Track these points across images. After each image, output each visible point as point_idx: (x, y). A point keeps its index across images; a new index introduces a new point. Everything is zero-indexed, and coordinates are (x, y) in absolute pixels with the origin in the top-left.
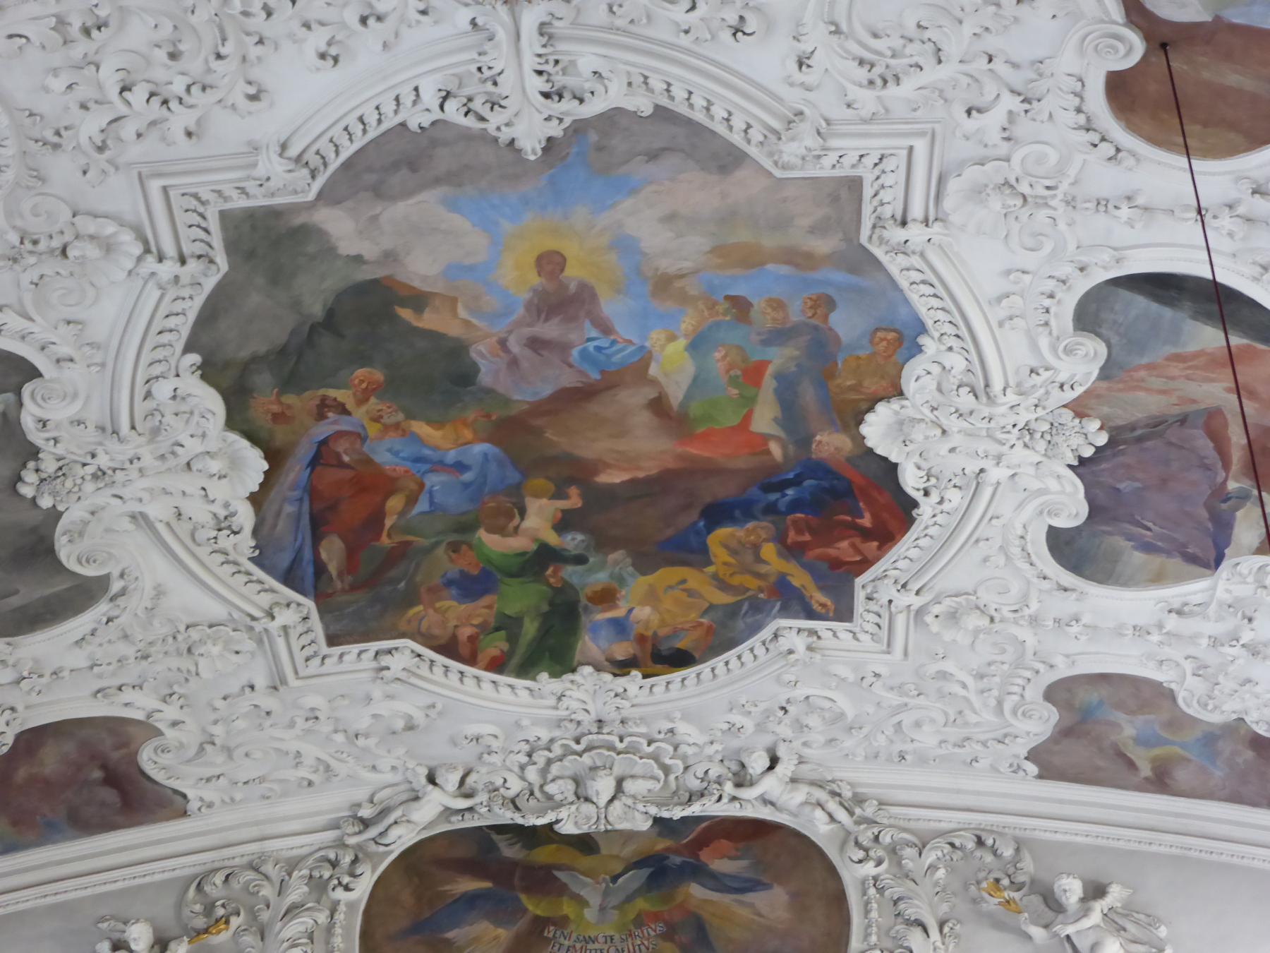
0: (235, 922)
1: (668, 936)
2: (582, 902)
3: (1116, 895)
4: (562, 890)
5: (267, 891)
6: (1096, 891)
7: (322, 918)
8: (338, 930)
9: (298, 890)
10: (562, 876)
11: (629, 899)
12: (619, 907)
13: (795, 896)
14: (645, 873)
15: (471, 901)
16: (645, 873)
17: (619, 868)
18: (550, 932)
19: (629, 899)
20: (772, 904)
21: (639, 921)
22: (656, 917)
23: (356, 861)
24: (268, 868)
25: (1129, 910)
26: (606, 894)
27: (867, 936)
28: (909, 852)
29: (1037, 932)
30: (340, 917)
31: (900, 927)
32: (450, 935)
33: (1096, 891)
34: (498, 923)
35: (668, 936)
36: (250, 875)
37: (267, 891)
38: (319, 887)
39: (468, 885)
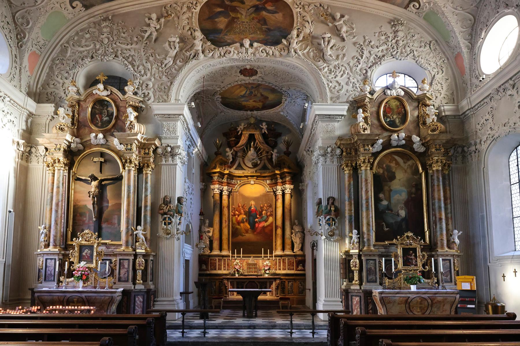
0: (173, 15)
1: (259, 22)
2: (242, 14)
3: (346, 17)
4: (238, 12)
5: (179, 9)
6: (342, 16)
7: (190, 15)
8: (193, 18)
9: (185, 9)
10: (237, 8)
11: (251, 14)
12: (249, 16)
13: (283, 15)
14: (254, 9)
15: (220, 13)
16: (254, 9)
17: (249, 7)
18: (236, 20)
19: (251, 14)
20: (279, 16)
21: (253, 19)
22: (257, 18)
23: (196, 3)
24: (179, 4)
25: (348, 20)
26: (246, 13)
27: (297, 23)
28: (306, 7)
29: (330, 24)
30: (194, 15)
31: (304, 22)
32: (216, 20)
33: (342, 16)
34: (225, 18)
35: (259, 22)
36: (175, 5)
37: (179, 9)
38: (189, 8)
39: (219, 10)
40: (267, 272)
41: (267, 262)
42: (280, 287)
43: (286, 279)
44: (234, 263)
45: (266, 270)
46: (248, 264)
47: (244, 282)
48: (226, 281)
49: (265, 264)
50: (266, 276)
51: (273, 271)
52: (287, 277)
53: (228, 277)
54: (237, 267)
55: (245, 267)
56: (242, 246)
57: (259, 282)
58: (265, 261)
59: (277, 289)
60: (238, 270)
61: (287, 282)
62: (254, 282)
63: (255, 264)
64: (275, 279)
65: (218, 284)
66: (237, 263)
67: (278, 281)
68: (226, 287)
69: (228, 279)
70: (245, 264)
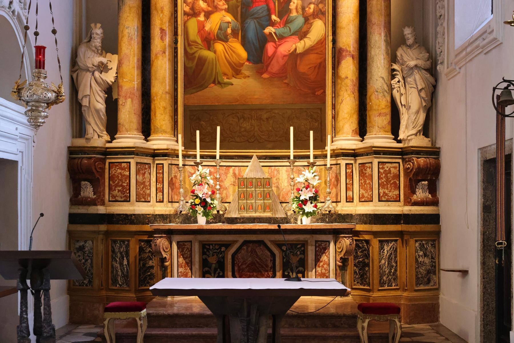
40: (309, 208)
41: (308, 174)
42: (351, 258)
43: (375, 234)
44: (193, 178)
45: (305, 202)
46: (243, 183)
47: (228, 245)
48: (162, 242)
49: (301, 179)
50: (306, 222)
51: (326, 206)
52: (376, 228)
53: (173, 226)
54: (203, 192)
55: (232, 193)
56: (213, 123)
57: (279, 245)
58: (299, 173)
59: (343, 265)
60: (204, 203)
61: (375, 243)
62: (262, 243)
63: (267, 182)
64: (336, 233)
65: (134, 248)
66: (203, 177)
67: (346, 242)
68: (163, 260)
69: (170, 233)
70: (229, 181)
